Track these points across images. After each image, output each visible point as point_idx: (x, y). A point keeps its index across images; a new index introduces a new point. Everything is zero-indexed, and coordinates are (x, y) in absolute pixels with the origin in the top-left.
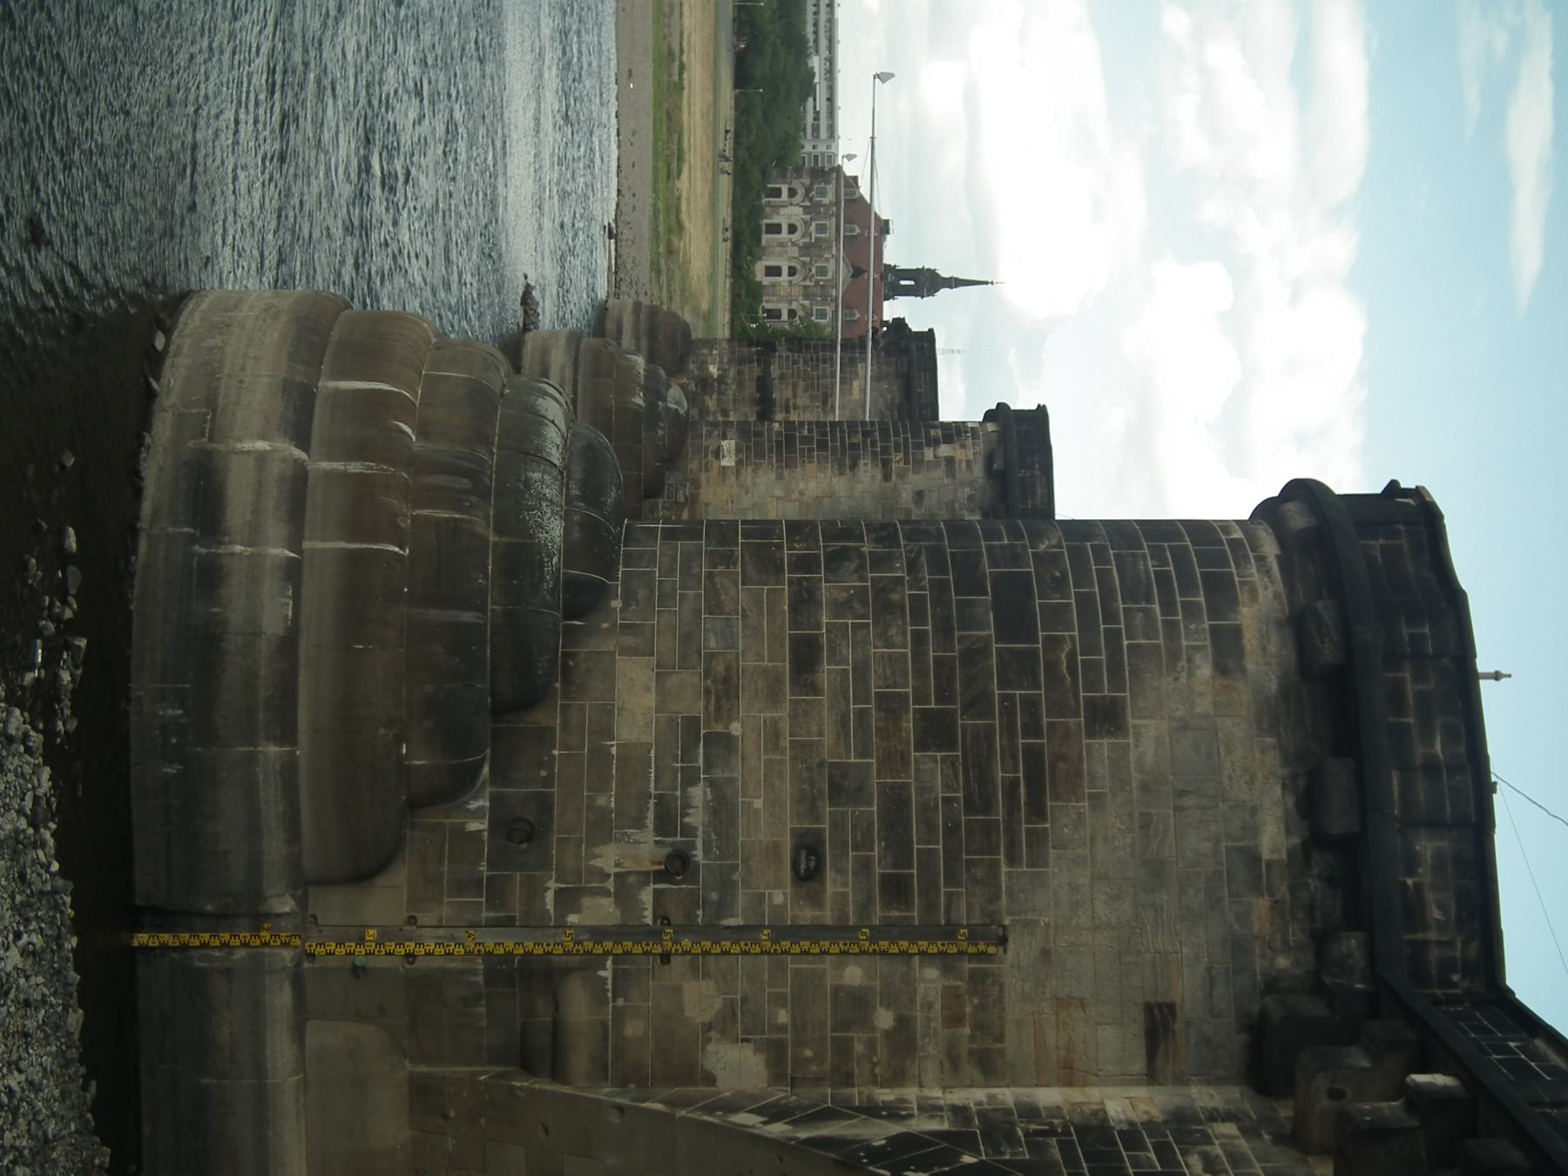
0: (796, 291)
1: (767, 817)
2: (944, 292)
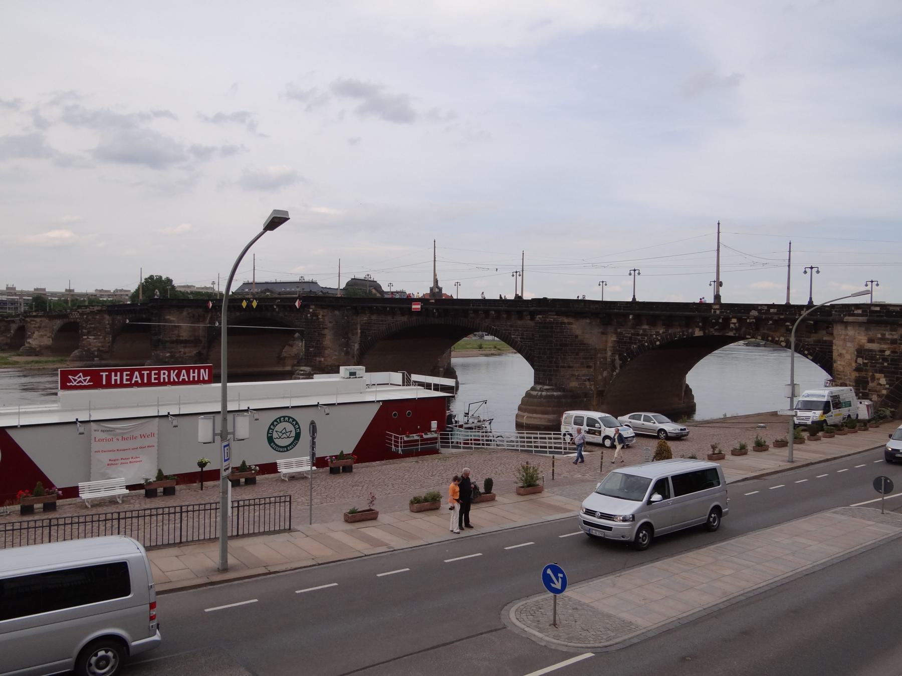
1: (585, 371)
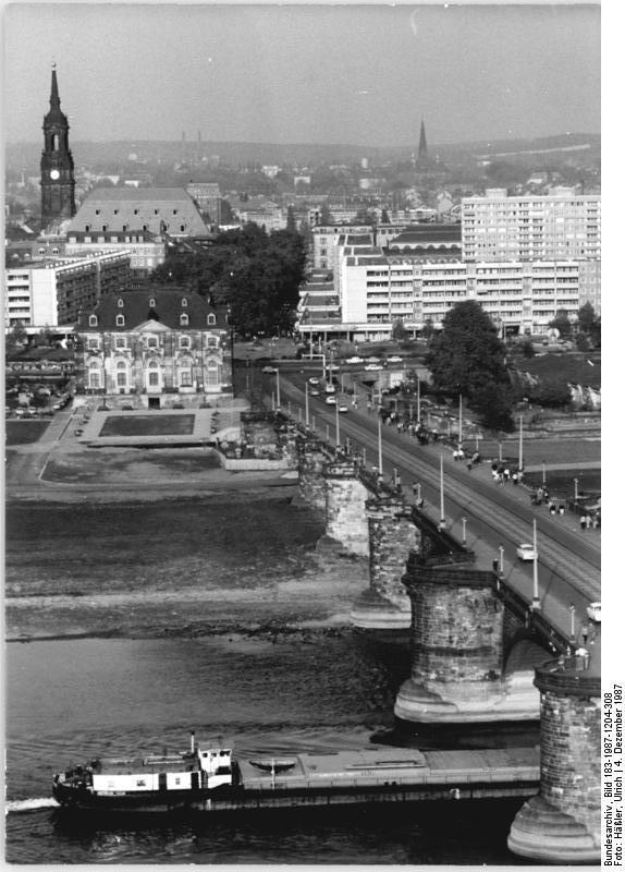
0: (169, 362)
2: (64, 108)
